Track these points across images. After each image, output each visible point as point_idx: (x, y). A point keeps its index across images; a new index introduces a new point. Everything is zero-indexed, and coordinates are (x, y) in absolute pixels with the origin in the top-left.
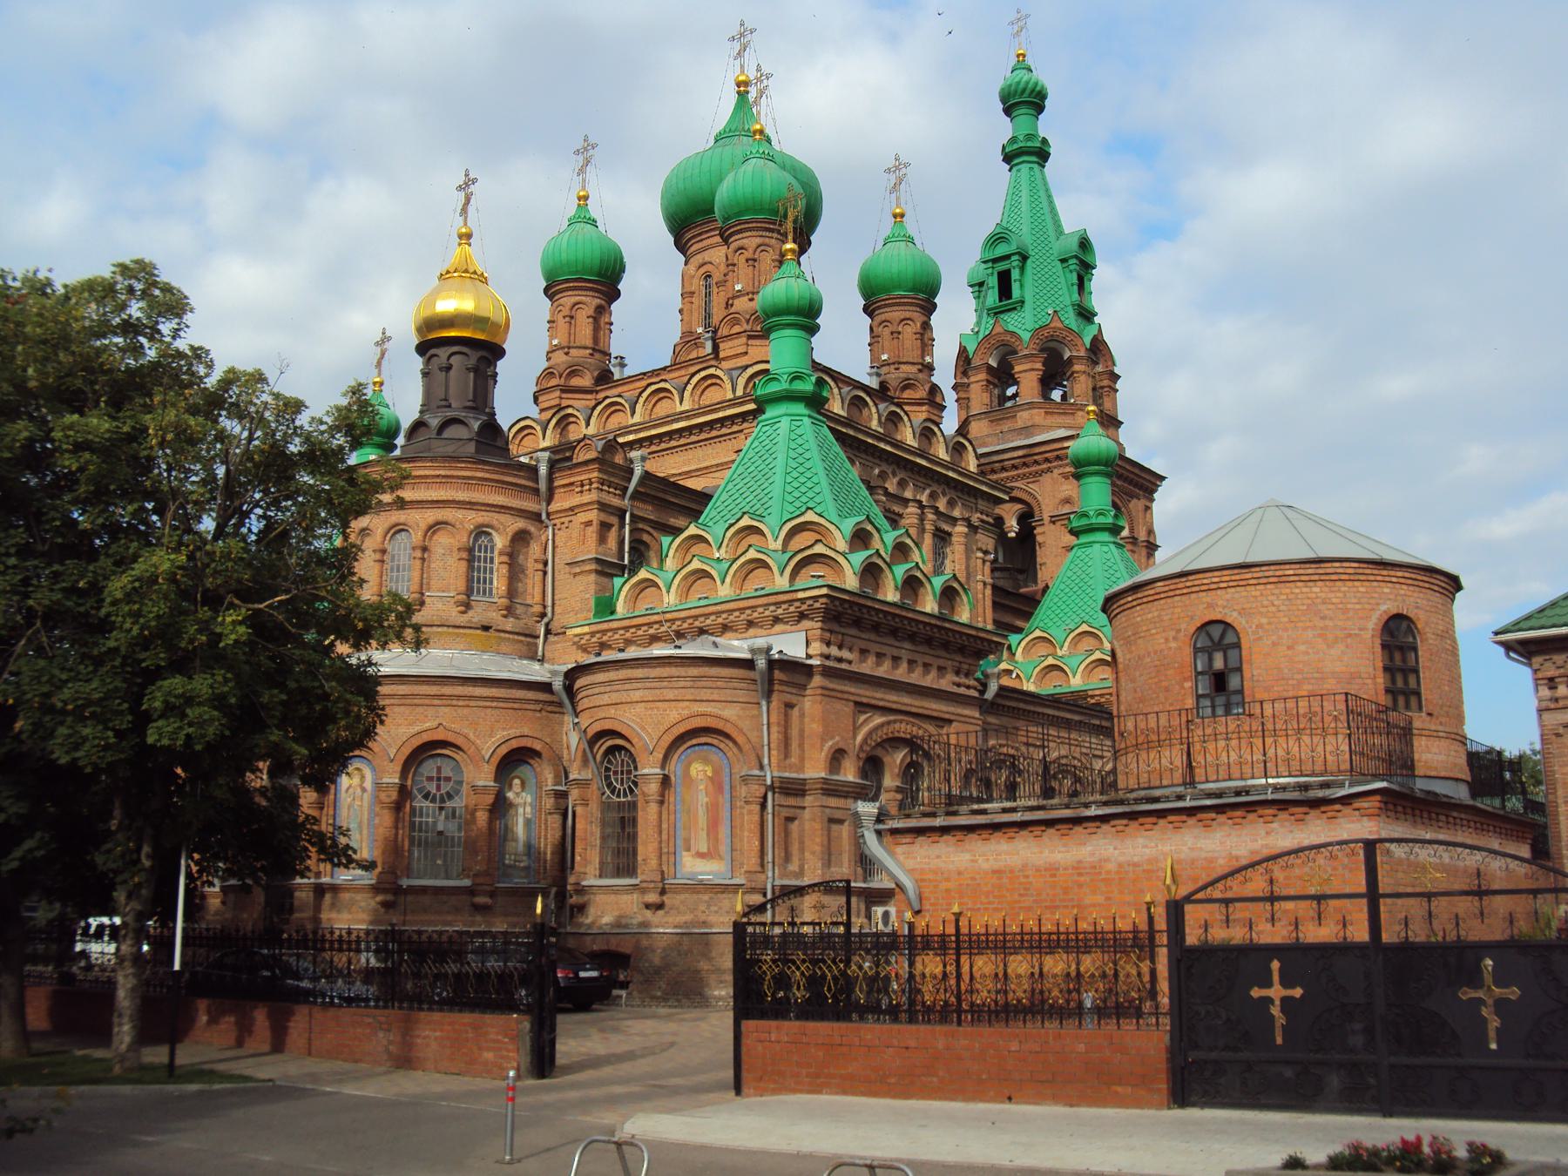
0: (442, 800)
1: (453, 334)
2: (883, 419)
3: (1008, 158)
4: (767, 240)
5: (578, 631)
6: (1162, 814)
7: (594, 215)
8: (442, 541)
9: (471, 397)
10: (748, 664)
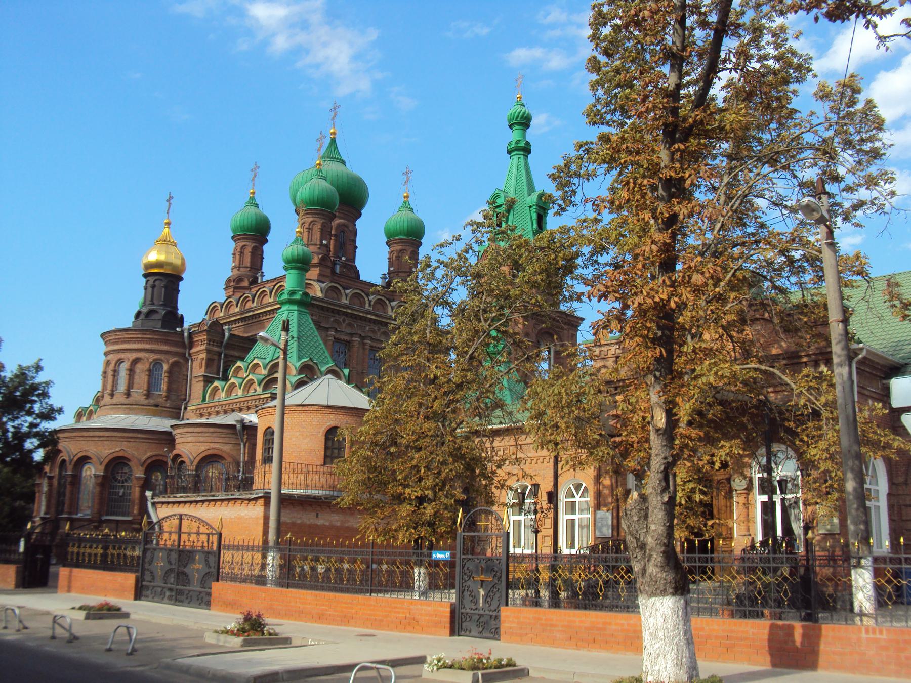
0: (123, 482)
1: (156, 271)
2: (372, 303)
3: (509, 152)
4: (316, 219)
5: (191, 408)
6: (216, 501)
7: (257, 202)
8: (139, 367)
9: (163, 299)
10: (233, 427)
